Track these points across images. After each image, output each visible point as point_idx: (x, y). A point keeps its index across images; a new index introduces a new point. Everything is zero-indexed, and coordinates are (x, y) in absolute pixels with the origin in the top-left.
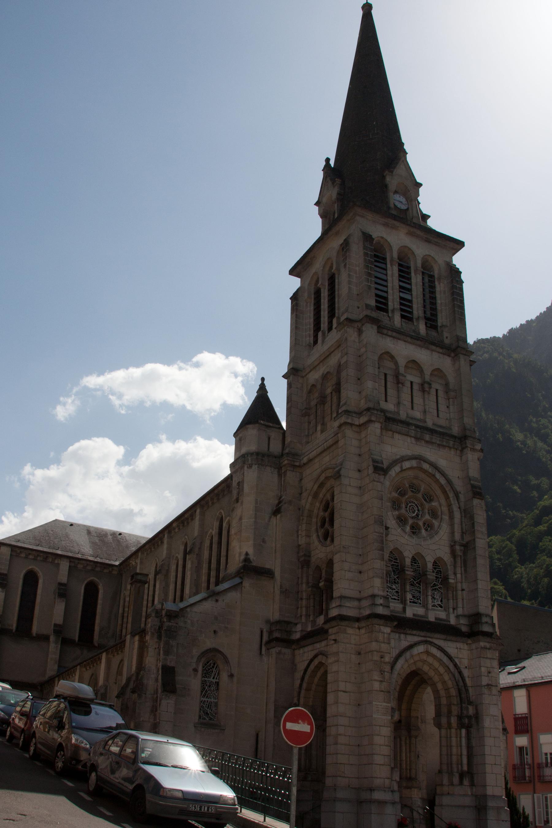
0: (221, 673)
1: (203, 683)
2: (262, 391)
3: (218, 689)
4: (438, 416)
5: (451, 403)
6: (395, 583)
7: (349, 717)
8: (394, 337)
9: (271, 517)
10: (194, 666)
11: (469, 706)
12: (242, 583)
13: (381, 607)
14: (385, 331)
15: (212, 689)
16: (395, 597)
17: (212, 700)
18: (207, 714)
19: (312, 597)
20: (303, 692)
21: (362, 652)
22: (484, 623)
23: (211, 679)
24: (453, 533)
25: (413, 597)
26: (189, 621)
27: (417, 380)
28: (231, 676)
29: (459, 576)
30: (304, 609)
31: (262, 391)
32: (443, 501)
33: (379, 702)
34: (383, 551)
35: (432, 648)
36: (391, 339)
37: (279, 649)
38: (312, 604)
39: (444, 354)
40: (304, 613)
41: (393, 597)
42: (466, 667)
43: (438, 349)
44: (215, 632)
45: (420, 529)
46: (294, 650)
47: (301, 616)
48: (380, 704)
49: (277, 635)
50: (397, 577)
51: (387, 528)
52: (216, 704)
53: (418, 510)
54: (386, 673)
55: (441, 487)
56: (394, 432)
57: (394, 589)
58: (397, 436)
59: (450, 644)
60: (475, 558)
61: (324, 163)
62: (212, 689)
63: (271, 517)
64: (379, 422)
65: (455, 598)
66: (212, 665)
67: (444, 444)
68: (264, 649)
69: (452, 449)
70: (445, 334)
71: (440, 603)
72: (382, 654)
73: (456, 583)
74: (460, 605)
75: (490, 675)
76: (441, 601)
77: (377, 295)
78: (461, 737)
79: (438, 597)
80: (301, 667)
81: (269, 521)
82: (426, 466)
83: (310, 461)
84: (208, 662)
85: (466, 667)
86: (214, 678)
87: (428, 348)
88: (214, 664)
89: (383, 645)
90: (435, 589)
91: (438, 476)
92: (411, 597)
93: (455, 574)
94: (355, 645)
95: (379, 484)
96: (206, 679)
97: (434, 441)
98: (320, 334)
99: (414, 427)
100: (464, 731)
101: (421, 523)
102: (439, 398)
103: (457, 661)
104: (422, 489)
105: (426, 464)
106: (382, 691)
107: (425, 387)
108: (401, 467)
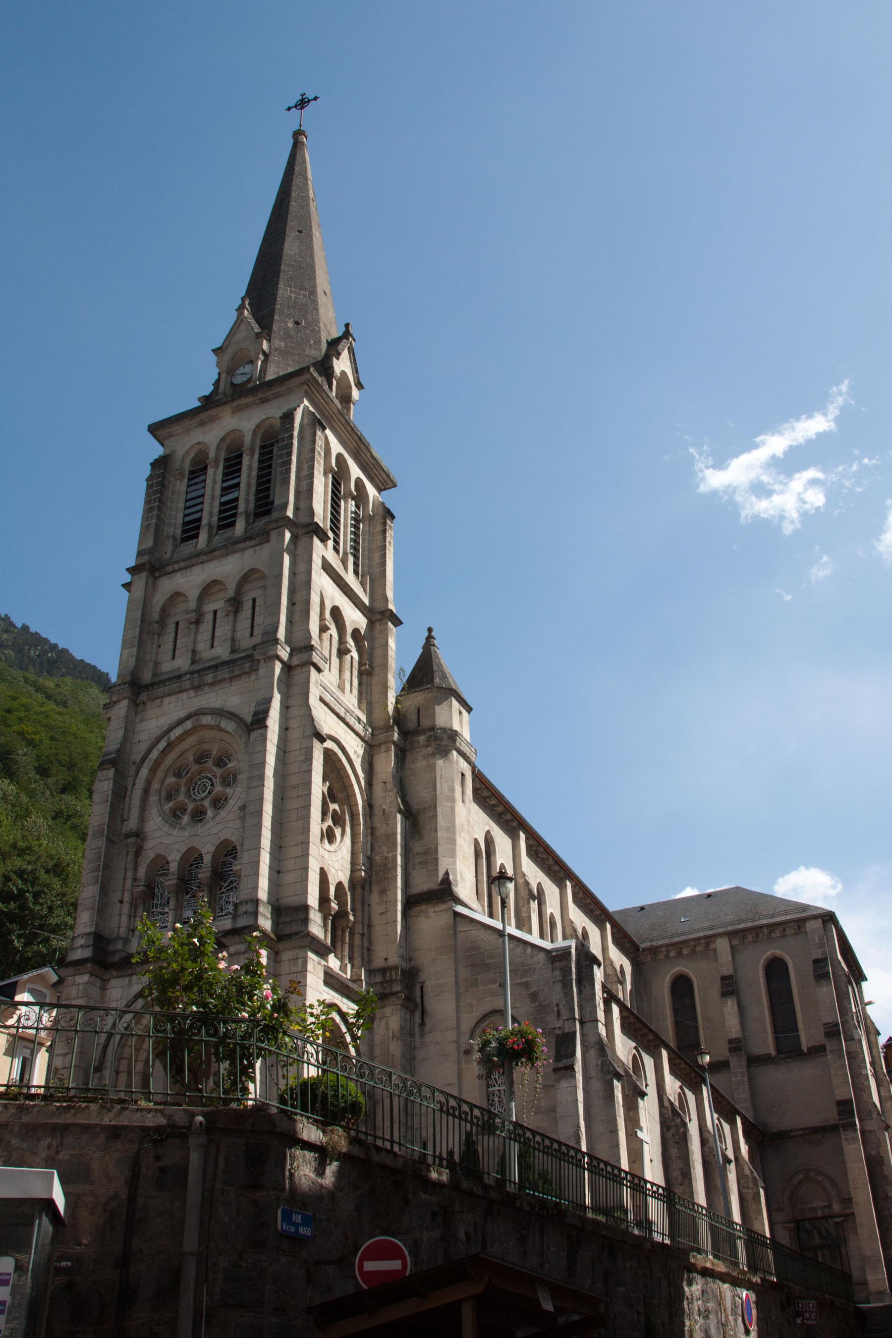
8: (186, 568)
14: (170, 569)
36: (182, 572)
39: (262, 544)
43: (248, 543)
53: (212, 785)
56: (163, 697)
58: (167, 700)
64: (125, 698)
67: (237, 673)
82: (207, 720)
87: (235, 552)
95: (106, 782)
97: (220, 677)
101: (206, 803)
102: (257, 609)
104: (214, 753)
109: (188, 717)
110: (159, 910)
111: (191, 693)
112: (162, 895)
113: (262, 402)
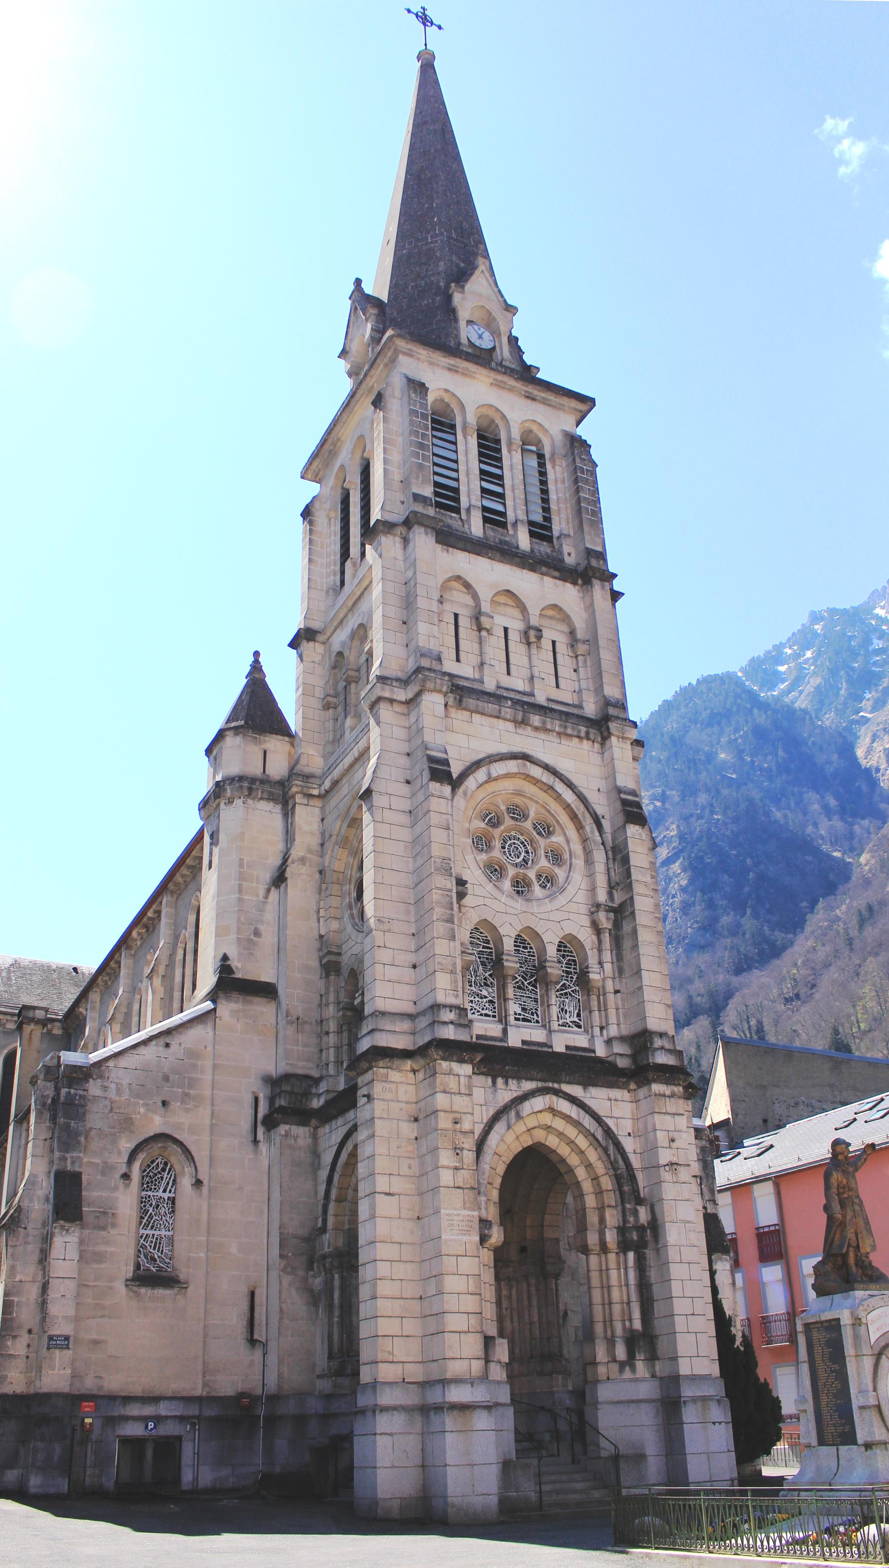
0: (178, 1181)
1: (143, 1202)
2: (256, 672)
3: (173, 1211)
4: (558, 686)
5: (580, 664)
6: (486, 985)
7: (400, 1243)
9: (268, 891)
10: (123, 1169)
11: (638, 1208)
12: (215, 1010)
13: (451, 1027)
15: (162, 1211)
16: (487, 1012)
17: (163, 1233)
18: (153, 1259)
19: (345, 1028)
20: (332, 1206)
21: (420, 1117)
22: (658, 1049)
23: (160, 1193)
24: (593, 890)
25: (524, 1009)
26: (113, 1086)
27: (516, 626)
28: (198, 1183)
29: (608, 967)
30: (332, 1051)
31: (256, 672)
32: (572, 833)
33: (455, 1209)
34: (453, 923)
35: (561, 1101)
37: (287, 1127)
38: (345, 1042)
40: (332, 1059)
41: (484, 1012)
42: (629, 1134)
44: (164, 1103)
45: (529, 885)
46: (316, 1128)
47: (327, 1065)
48: (456, 1212)
49: (282, 1102)
50: (490, 975)
51: (461, 882)
52: (171, 1240)
53: (527, 852)
54: (465, 1152)
55: (567, 807)
57: (486, 997)
58: (477, 718)
59: (594, 1091)
60: (635, 932)
61: (353, 287)
62: (162, 1211)
63: (268, 891)
65: (603, 1008)
66: (161, 1166)
67: (569, 731)
68: (261, 1130)
69: (585, 741)
70: (566, 549)
71: (576, 1019)
72: (458, 1115)
73: (604, 980)
74: (613, 1019)
75: (674, 1145)
76: (579, 1015)
77: (437, 484)
78: (626, 1269)
79: (572, 1008)
80: (327, 1158)
81: (266, 897)
83: (335, 783)
84: (153, 1162)
85: (629, 1134)
86: (165, 1191)
88: (166, 1164)
89: (457, 1099)
90: (566, 994)
91: (560, 787)
92: (519, 1011)
93: (601, 963)
94: (407, 1103)
96: (150, 1193)
98: (348, 564)
99: (509, 703)
100: (631, 1255)
101: (532, 874)
103: (610, 1123)
104: (532, 814)
105: (536, 767)
106: (459, 1188)
107: (532, 635)
108: (489, 774)
109: (513, 756)
110: (473, 988)
111: (510, 726)
112: (475, 971)
113: (527, 397)
